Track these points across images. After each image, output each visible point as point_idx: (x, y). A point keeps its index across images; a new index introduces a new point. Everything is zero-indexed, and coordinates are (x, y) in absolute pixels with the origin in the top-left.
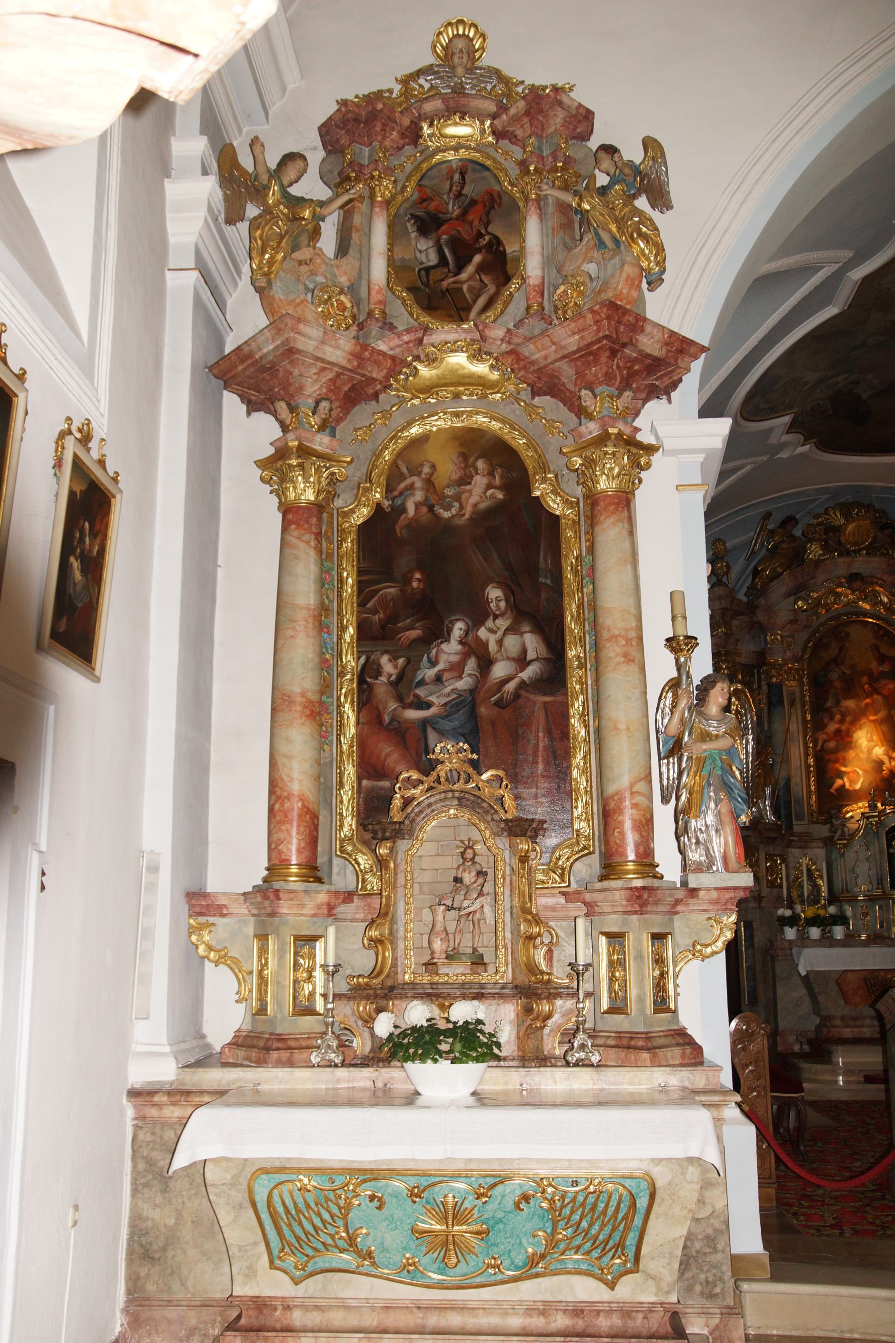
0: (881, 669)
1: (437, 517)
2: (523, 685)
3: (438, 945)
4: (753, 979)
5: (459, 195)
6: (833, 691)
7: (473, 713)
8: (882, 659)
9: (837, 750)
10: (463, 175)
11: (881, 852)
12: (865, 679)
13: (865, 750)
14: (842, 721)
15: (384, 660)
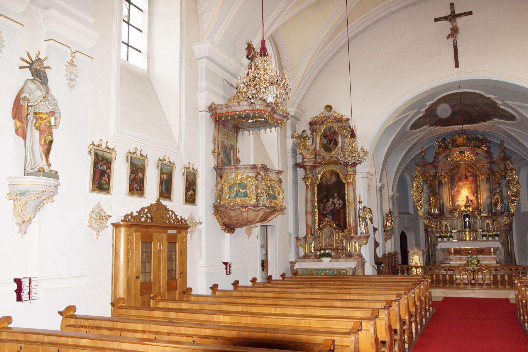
1: (328, 184)
2: (340, 208)
3: (327, 244)
4: (431, 250)
5: (330, 132)
6: (456, 181)
7: (333, 212)
10: (330, 128)
11: (462, 220)
14: (458, 188)
15: (321, 205)
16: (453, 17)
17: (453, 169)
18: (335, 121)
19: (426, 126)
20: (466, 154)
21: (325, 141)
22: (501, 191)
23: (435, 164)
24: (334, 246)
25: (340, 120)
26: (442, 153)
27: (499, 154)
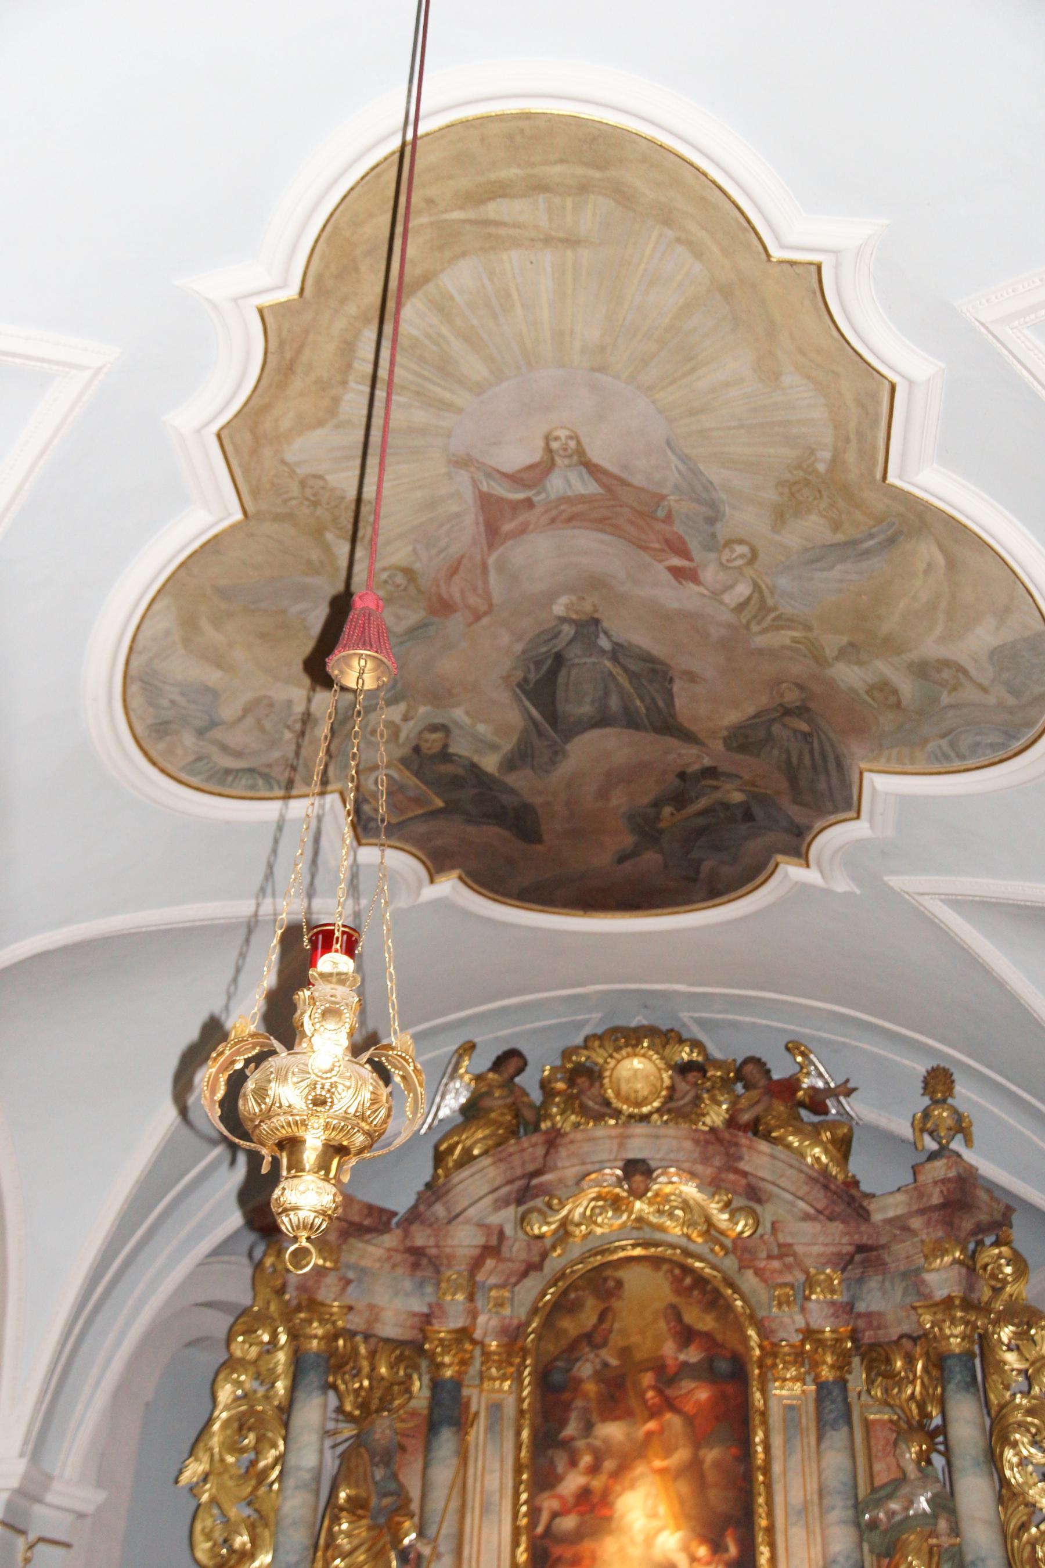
0: (682, 1357)
6: (579, 1403)
8: (686, 1335)
9: (577, 1536)
12: (648, 1379)
13: (640, 1538)
14: (594, 1469)
17: (563, 1306)
23: (421, 1238)
27: (915, 1170)
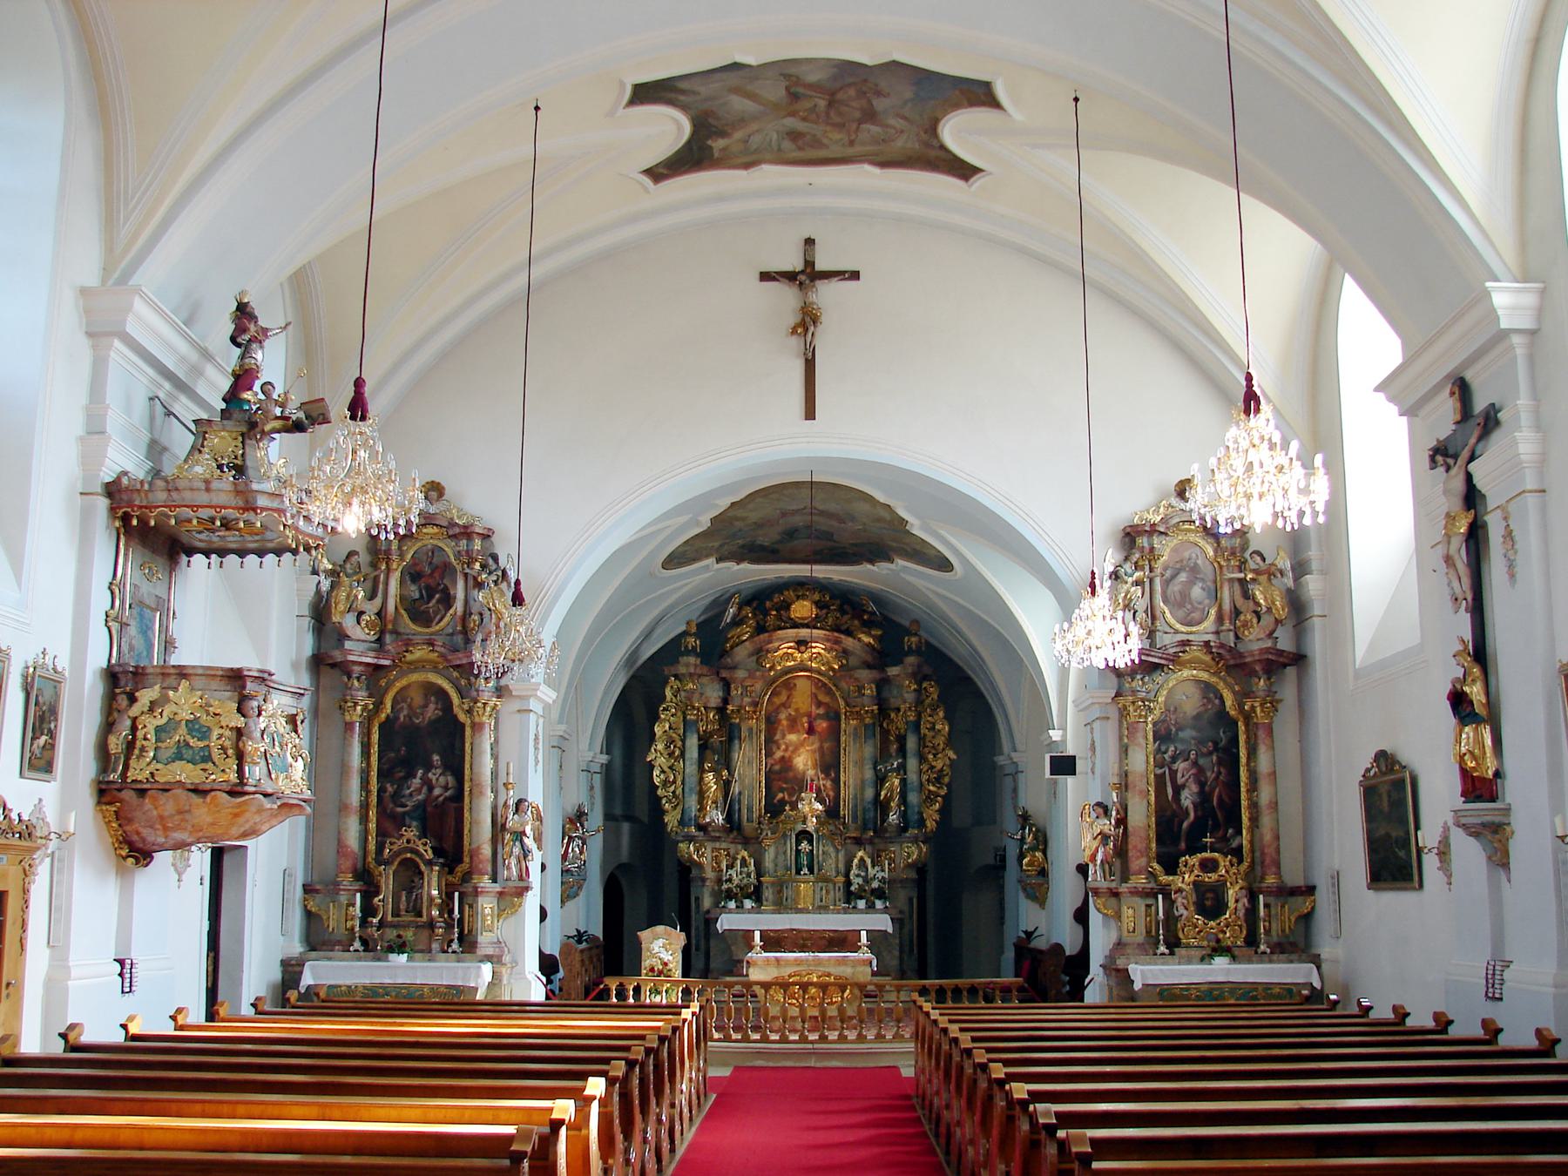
1: (413, 722)
2: (446, 799)
5: (431, 563)
6: (781, 728)
7: (425, 810)
8: (819, 704)
15: (388, 785)
16: (807, 276)
18: (451, 533)
19: (711, 561)
20: (814, 651)
21: (414, 591)
22: (902, 768)
24: (421, 916)
25: (467, 533)
26: (747, 643)
